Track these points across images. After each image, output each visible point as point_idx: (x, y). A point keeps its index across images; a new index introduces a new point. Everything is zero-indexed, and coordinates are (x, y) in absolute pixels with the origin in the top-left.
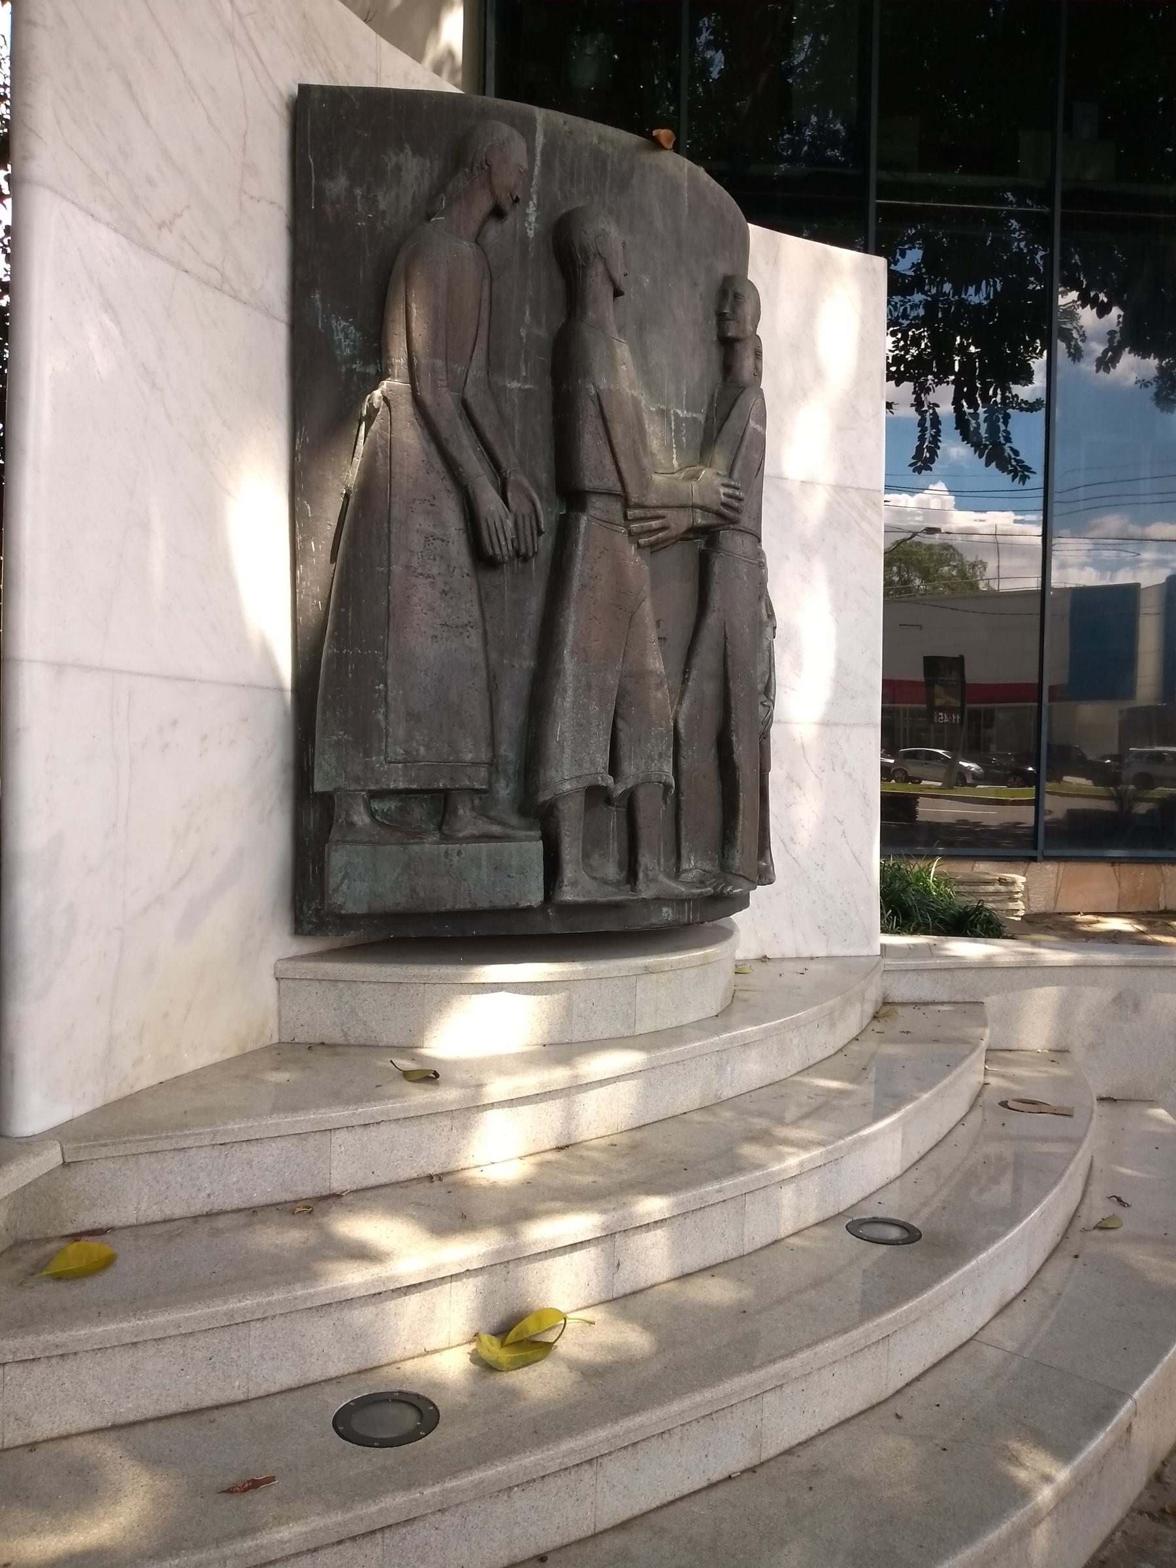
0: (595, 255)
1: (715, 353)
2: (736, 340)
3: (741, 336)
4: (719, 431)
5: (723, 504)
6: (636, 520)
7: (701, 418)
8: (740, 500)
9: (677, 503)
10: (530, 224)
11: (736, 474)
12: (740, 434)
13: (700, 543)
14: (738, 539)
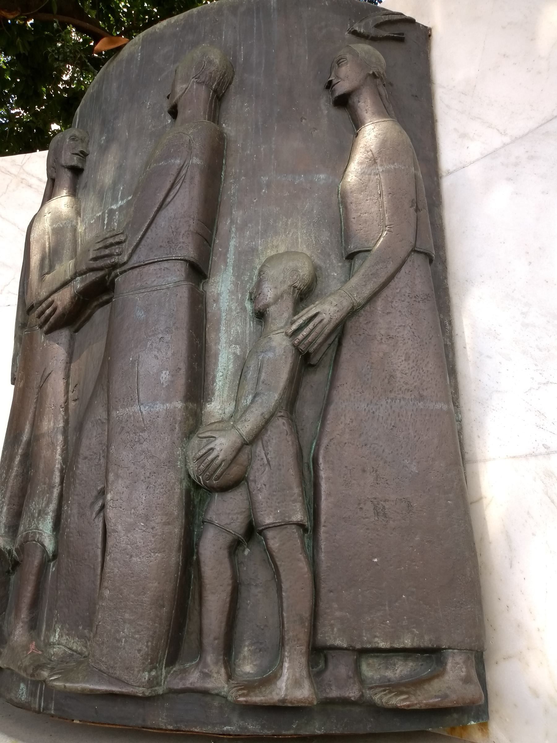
5: (95, 259)
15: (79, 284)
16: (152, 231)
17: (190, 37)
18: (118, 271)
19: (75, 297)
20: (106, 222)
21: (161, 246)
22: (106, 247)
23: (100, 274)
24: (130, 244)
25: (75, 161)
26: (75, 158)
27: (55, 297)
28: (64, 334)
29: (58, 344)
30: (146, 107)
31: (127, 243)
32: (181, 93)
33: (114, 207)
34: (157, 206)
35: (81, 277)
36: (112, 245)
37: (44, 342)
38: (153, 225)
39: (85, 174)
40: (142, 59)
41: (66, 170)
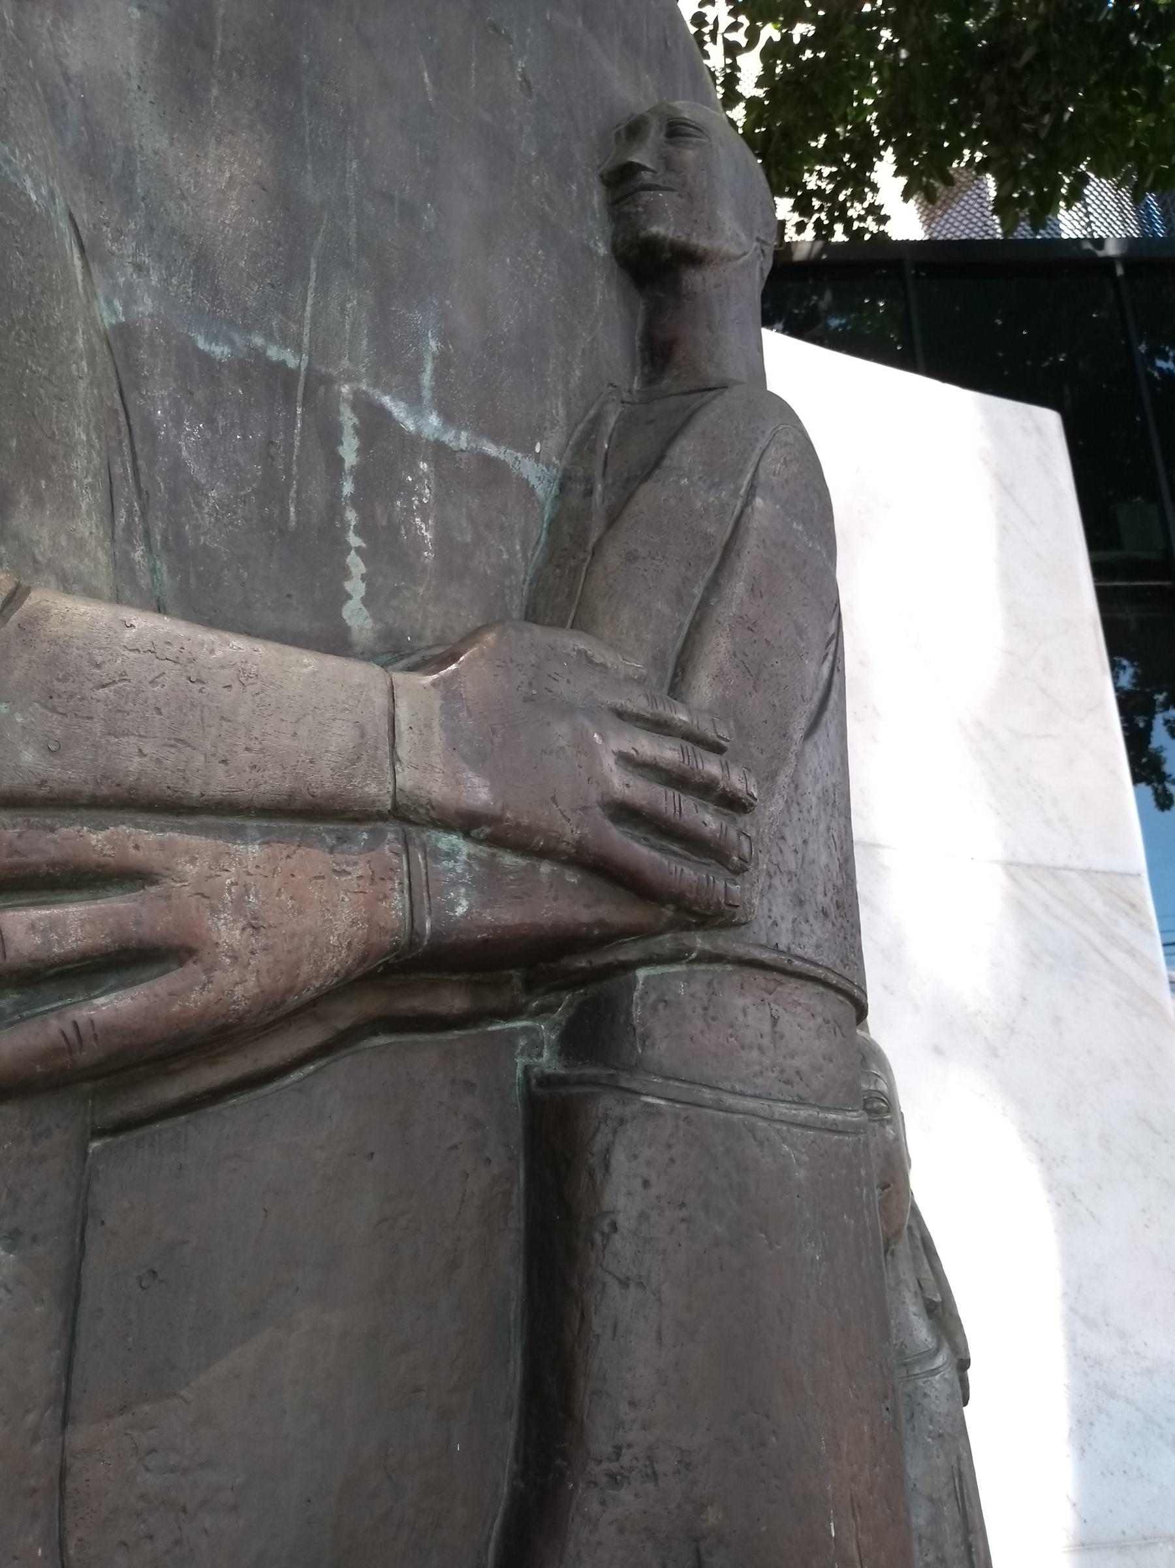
2: (690, 258)
3: (702, 243)
4: (613, 518)
5: (625, 813)
7: (536, 471)
8: (733, 804)
9: (271, 783)
11: (704, 687)
12: (719, 532)
13: (533, 1042)
14: (747, 1007)
15: (462, 895)
18: (699, 942)
20: (349, 451)
22: (677, 780)
32: (734, 250)
33: (398, 410)
35: (483, 851)
36: (706, 790)
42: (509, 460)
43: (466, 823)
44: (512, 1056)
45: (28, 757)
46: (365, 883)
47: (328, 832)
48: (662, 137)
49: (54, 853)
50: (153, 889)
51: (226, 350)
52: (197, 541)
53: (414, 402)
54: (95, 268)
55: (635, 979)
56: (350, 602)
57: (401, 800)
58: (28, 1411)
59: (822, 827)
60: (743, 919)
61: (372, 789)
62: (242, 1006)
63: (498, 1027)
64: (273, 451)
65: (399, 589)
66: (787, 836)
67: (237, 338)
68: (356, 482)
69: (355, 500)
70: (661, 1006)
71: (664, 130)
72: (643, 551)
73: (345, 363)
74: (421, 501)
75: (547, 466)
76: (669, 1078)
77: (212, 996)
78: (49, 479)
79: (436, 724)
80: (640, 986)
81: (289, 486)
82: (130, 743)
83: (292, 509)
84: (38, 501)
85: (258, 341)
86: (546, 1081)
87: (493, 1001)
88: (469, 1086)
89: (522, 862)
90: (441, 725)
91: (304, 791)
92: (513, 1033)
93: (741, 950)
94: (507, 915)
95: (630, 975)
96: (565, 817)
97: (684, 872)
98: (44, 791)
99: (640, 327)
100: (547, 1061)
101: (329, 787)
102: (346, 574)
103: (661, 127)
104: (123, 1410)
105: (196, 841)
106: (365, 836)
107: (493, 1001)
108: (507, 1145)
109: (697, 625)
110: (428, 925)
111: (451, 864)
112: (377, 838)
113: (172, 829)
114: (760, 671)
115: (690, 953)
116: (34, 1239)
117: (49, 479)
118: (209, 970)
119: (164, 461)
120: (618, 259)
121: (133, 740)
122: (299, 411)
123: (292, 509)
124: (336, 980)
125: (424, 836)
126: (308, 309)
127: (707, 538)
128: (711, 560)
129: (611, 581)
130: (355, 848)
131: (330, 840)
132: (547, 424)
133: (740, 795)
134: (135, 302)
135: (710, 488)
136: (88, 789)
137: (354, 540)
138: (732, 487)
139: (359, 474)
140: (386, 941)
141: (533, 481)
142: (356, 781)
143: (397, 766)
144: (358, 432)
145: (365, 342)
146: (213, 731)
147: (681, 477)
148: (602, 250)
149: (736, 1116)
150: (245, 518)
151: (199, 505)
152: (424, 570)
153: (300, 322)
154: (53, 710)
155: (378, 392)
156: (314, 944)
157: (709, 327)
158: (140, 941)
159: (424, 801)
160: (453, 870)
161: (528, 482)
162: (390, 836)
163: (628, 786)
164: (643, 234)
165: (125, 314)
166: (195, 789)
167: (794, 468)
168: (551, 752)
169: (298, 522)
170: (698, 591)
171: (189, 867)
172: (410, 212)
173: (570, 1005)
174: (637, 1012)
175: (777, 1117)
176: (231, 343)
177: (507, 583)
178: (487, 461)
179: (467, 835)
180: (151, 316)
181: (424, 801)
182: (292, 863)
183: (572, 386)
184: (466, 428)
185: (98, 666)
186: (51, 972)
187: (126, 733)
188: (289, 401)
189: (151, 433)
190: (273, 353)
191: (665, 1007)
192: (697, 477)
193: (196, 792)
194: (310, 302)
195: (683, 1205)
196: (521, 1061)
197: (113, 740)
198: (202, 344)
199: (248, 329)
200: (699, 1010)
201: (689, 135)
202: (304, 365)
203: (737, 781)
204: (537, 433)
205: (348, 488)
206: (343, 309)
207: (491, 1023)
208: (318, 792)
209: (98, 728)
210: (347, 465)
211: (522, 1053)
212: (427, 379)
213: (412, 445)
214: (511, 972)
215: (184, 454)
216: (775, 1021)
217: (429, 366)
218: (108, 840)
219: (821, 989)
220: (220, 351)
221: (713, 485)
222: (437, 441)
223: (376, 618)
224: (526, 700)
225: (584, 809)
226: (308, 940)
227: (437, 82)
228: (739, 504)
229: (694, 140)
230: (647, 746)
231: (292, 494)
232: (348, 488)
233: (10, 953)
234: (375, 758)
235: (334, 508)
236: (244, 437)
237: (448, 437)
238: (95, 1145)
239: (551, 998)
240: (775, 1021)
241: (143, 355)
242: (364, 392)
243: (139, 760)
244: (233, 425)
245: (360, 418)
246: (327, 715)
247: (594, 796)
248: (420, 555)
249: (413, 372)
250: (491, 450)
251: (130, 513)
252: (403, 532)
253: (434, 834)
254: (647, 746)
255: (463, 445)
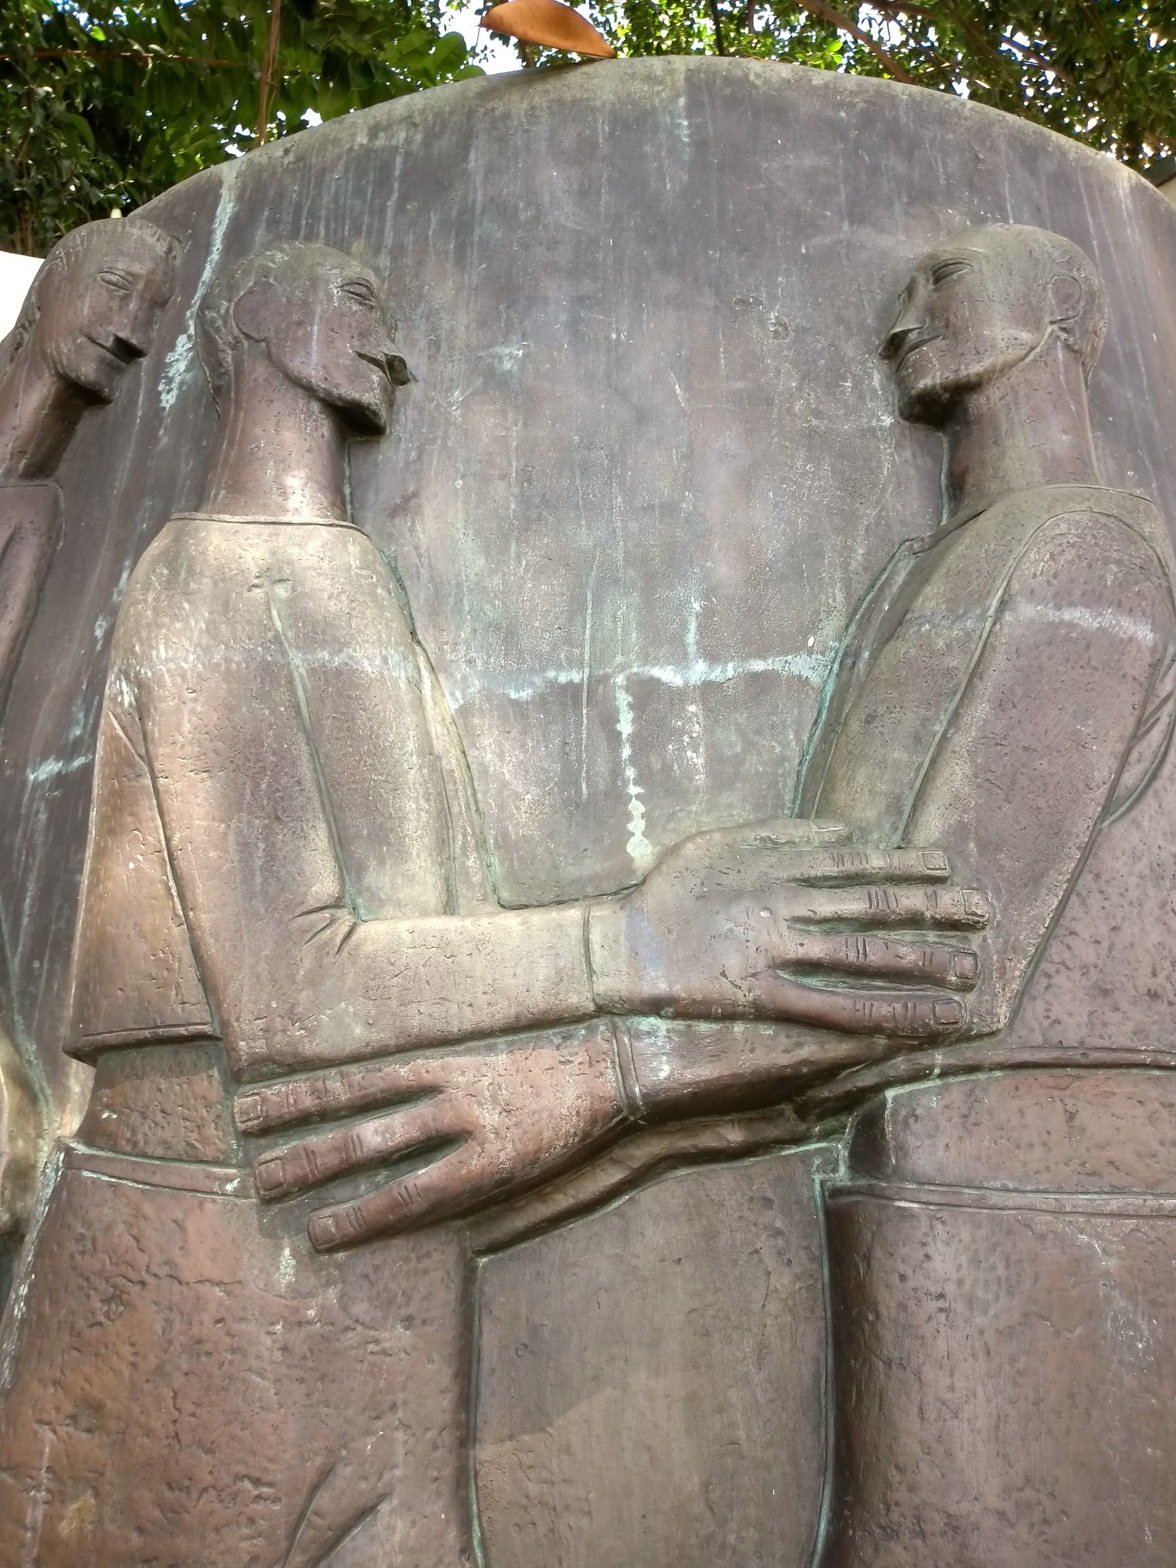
0: (235, 346)
1: (900, 469)
2: (962, 390)
3: (974, 369)
5: (806, 967)
6: (272, 1129)
7: (809, 666)
10: (170, 381)
11: (933, 823)
13: (826, 1160)
15: (664, 1062)
16: (1084, 903)
17: (893, 162)
18: (939, 1058)
19: (619, 1110)
20: (625, 726)
21: (1154, 995)
23: (838, 1049)
24: (1010, 948)
25: (368, 390)
26: (376, 376)
27: (458, 1069)
28: (427, 1270)
29: (408, 1321)
30: (762, 322)
31: (989, 932)
32: (1011, 354)
33: (667, 675)
34: (1101, 794)
35: (680, 1024)
36: (914, 921)
37: (296, 1292)
38: (1087, 879)
39: (391, 455)
40: (700, 144)
41: (315, 407)
42: (778, 666)
43: (655, 1006)
44: (808, 1173)
45: (358, 1030)
46: (586, 1067)
47: (554, 1034)
48: (931, 287)
49: (382, 1085)
50: (441, 1097)
51: (530, 691)
52: (517, 834)
53: (680, 659)
54: (441, 677)
55: (885, 1100)
56: (633, 840)
57: (601, 1002)
58: (427, 1429)
59: (1151, 905)
60: (986, 1030)
61: (574, 1000)
62: (507, 1165)
63: (793, 1151)
64: (567, 749)
65: (674, 813)
66: (1077, 927)
67: (537, 680)
68: (633, 747)
69: (633, 761)
70: (911, 1121)
71: (931, 280)
72: (881, 710)
73: (619, 659)
74: (691, 737)
75: (823, 654)
76: (924, 1184)
77: (485, 1161)
78: (389, 844)
79: (622, 938)
80: (889, 1105)
81: (580, 769)
82: (412, 1009)
83: (584, 786)
84: (382, 861)
85: (551, 674)
86: (837, 1192)
87: (771, 1132)
88: (768, 1203)
89: (715, 1027)
90: (626, 938)
91: (525, 1012)
92: (809, 1155)
93: (1000, 1056)
94: (705, 1072)
95: (881, 1096)
96: (736, 986)
97: (883, 1005)
98: (369, 1049)
99: (945, 467)
100: (842, 1175)
101: (542, 1005)
102: (629, 817)
103: (927, 280)
104: (511, 1437)
105: (463, 1060)
106: (583, 1032)
107: (771, 1132)
108: (807, 1248)
109: (933, 761)
110: (637, 1090)
111: (652, 1040)
112: (592, 1030)
113: (448, 1055)
114: (1013, 783)
115: (932, 1070)
116: (424, 1322)
117: (389, 844)
118: (482, 1144)
119: (493, 787)
120: (907, 418)
121: (414, 1006)
122: (585, 711)
123: (584, 786)
124: (577, 1139)
125: (628, 1023)
126: (588, 632)
127: (949, 672)
128: (955, 693)
129: (850, 747)
130: (576, 1043)
131: (557, 1040)
132: (823, 616)
133: (956, 917)
134: (469, 687)
135: (953, 623)
136: (392, 1042)
137: (634, 790)
138: (978, 612)
139: (635, 738)
140: (607, 1106)
141: (806, 673)
142: (561, 997)
143: (594, 978)
144: (631, 706)
145: (634, 635)
146: (462, 987)
147: (921, 625)
148: (887, 421)
149: (1005, 1212)
150: (551, 806)
151: (518, 808)
152: (697, 791)
153: (582, 646)
154: (369, 999)
155: (647, 668)
156: (551, 1116)
157: (996, 443)
158: (437, 1131)
159: (617, 999)
160: (655, 1043)
161: (800, 676)
162: (602, 1028)
163: (802, 945)
164: (914, 392)
165: (463, 698)
166: (454, 1028)
167: (1070, 554)
168: (720, 936)
169: (589, 795)
170: (939, 728)
171: (461, 1078)
172: (669, 509)
173: (852, 1127)
174: (889, 1128)
175: (1068, 1210)
176: (532, 684)
177: (780, 772)
178: (755, 677)
179: (661, 1017)
180: (479, 692)
181: (617, 999)
182: (529, 1062)
183: (854, 565)
184: (732, 659)
185: (393, 964)
186: (395, 1156)
187: (410, 1003)
188: (577, 705)
189: (485, 772)
190: (563, 678)
191: (916, 1121)
192: (940, 617)
193: (455, 1030)
194: (588, 626)
195: (941, 1296)
196: (817, 1178)
197: (403, 1008)
198: (514, 695)
199: (543, 669)
200: (957, 1119)
201: (952, 273)
202: (586, 676)
203: (950, 902)
204: (813, 627)
205: (626, 752)
206: (615, 617)
207: (782, 1149)
208: (535, 1011)
209: (394, 1003)
210: (624, 736)
211: (818, 1171)
212: (691, 637)
213: (678, 697)
214: (782, 1106)
215: (507, 776)
216: (1071, 1116)
217: (693, 626)
218: (410, 1070)
219: (1157, 1073)
220: (526, 694)
221: (958, 618)
222: (704, 681)
223: (654, 844)
224: (697, 898)
225: (754, 975)
226: (545, 1114)
227: (687, 388)
228: (988, 624)
229: (955, 276)
230: (827, 904)
231: (584, 775)
232: (626, 752)
233: (365, 1150)
234: (573, 977)
235: (616, 772)
236: (546, 747)
237: (716, 675)
238: (483, 1260)
239: (831, 1123)
240: (1071, 1116)
241: (476, 721)
242: (636, 674)
243: (422, 1018)
244: (538, 742)
245: (633, 695)
246: (536, 955)
247: (761, 963)
248: (691, 780)
249: (678, 640)
250: (758, 666)
251: (465, 836)
252: (676, 767)
253: (636, 1019)
254: (827, 904)
255: (730, 673)
